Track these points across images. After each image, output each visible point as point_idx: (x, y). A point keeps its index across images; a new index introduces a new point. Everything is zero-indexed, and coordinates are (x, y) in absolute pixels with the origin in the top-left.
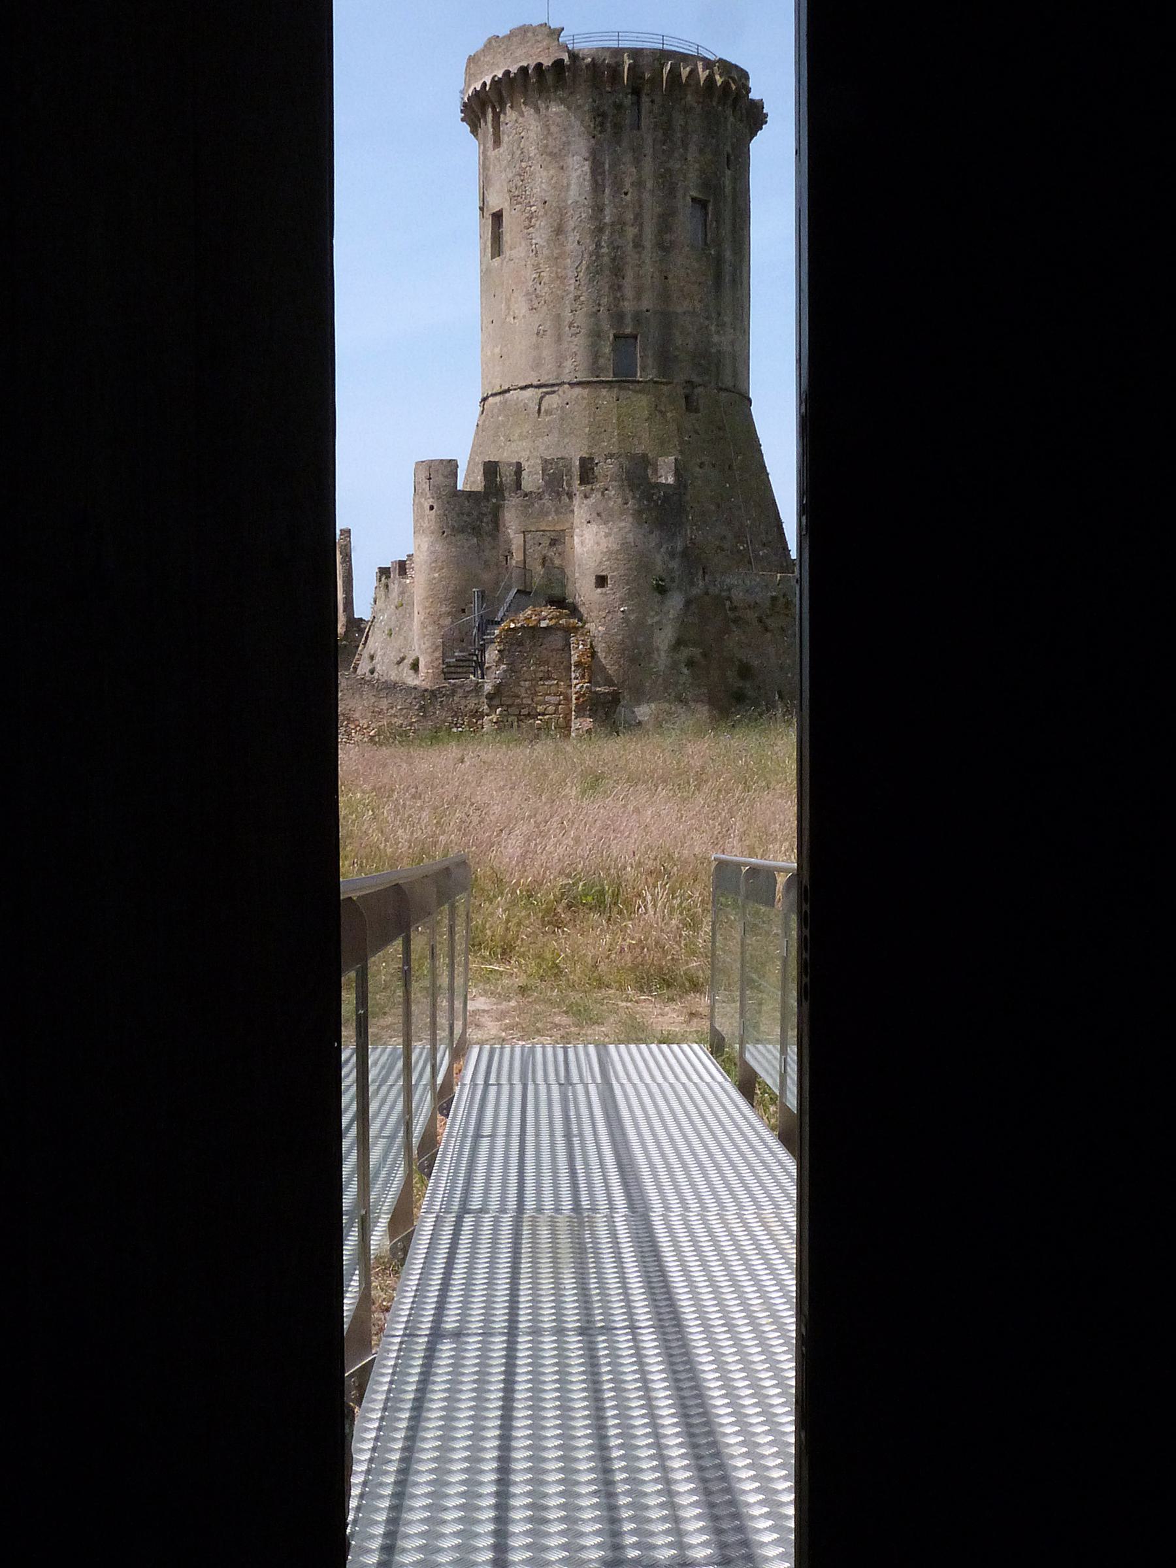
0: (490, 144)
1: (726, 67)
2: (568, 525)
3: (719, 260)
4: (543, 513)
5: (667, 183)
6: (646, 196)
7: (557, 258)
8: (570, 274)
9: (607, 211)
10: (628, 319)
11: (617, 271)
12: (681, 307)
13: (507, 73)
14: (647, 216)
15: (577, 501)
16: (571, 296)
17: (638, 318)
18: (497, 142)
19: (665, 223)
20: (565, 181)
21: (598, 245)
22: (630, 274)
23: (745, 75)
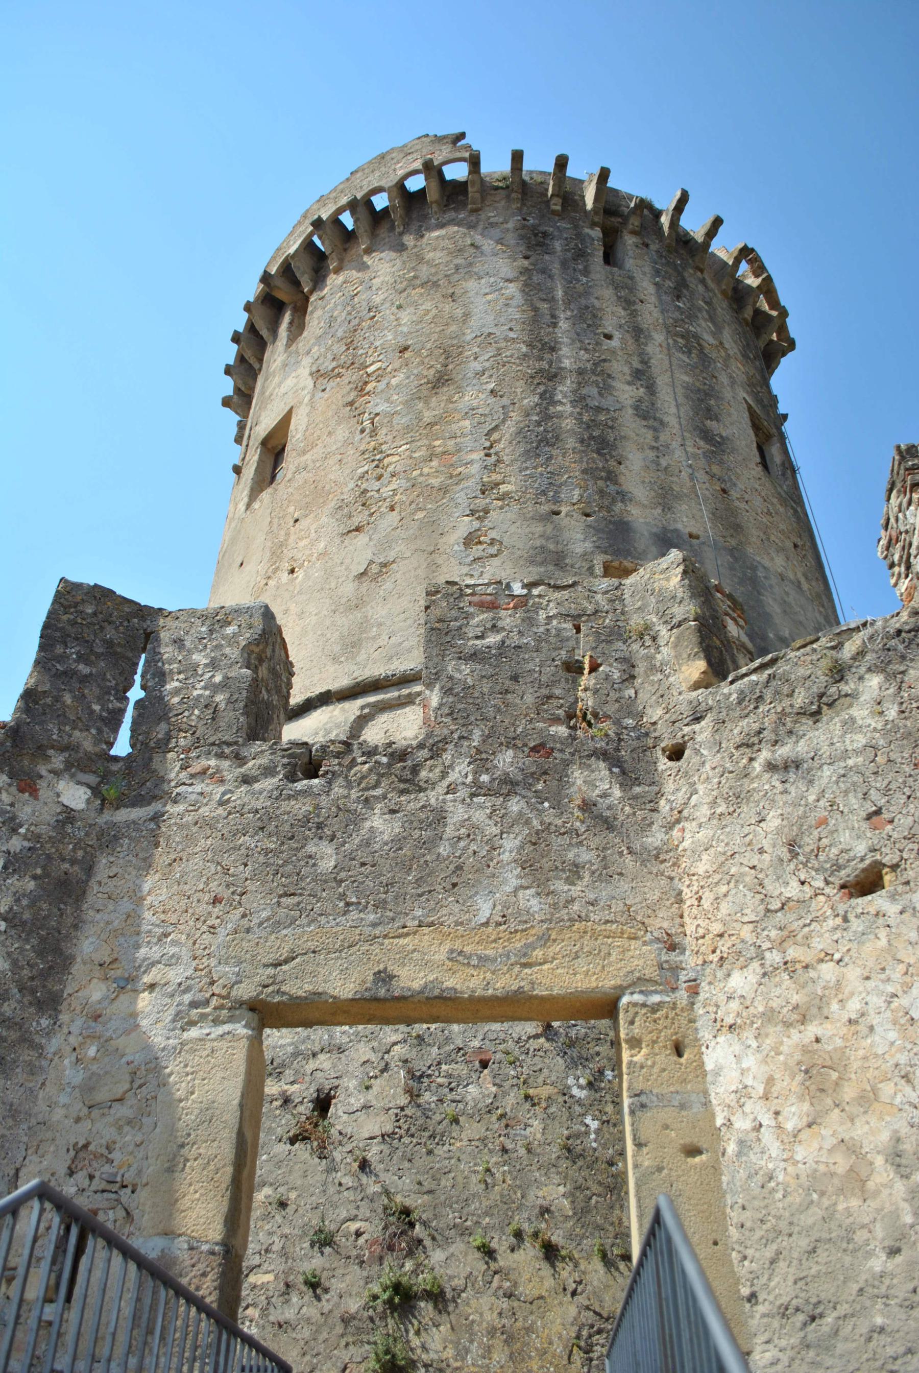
2: (642, 957)
4: (423, 873)
7: (431, 425)
8: (468, 442)
9: (565, 351)
11: (601, 442)
15: (692, 793)
16: (472, 484)
20: (459, 312)
21: (547, 398)
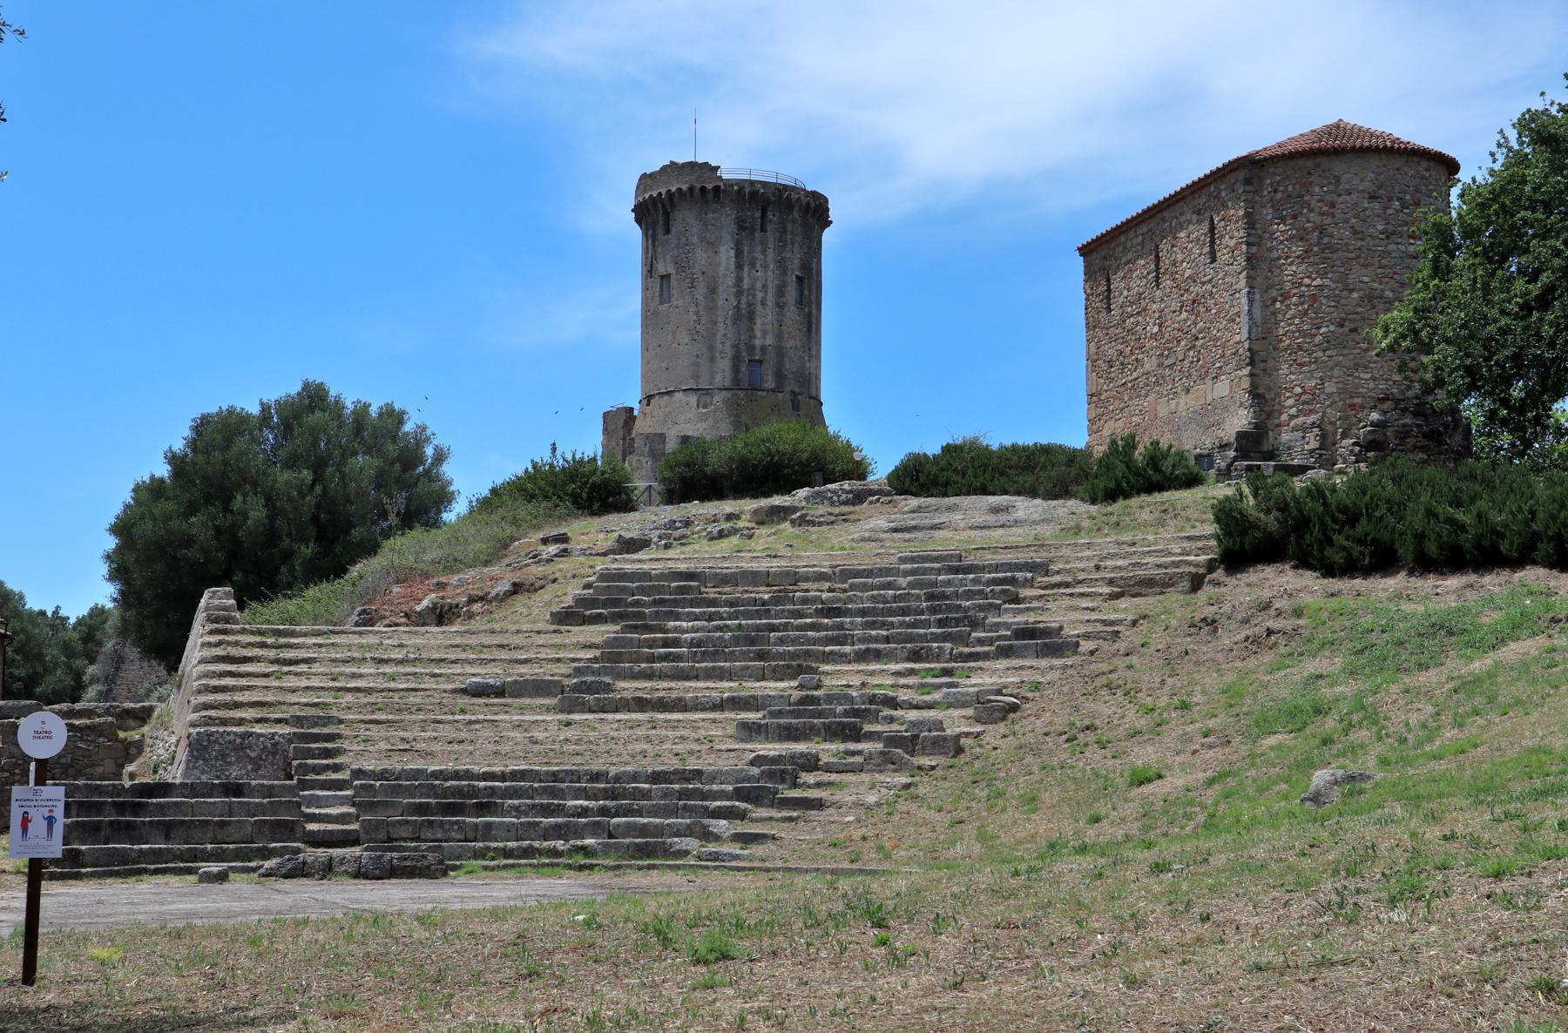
0: (660, 231)
1: (814, 193)
3: (810, 314)
5: (782, 267)
6: (770, 273)
10: (757, 351)
11: (751, 316)
12: (789, 344)
13: (680, 190)
14: (770, 286)
17: (763, 349)
18: (668, 231)
19: (781, 291)
22: (759, 321)
23: (826, 200)
